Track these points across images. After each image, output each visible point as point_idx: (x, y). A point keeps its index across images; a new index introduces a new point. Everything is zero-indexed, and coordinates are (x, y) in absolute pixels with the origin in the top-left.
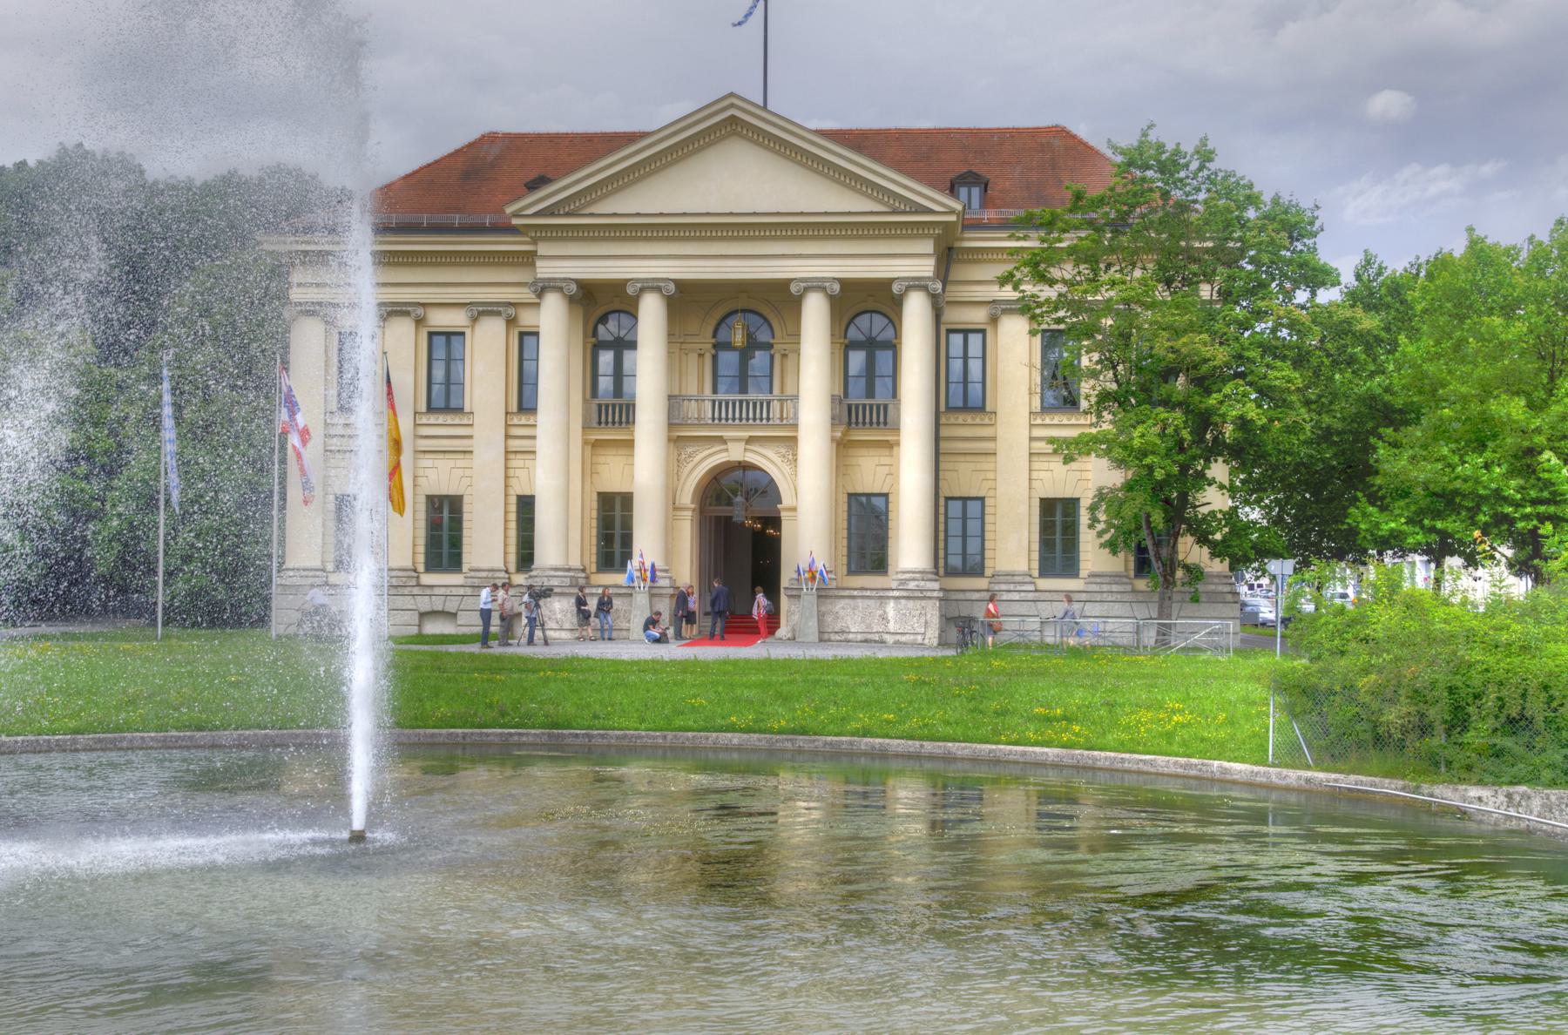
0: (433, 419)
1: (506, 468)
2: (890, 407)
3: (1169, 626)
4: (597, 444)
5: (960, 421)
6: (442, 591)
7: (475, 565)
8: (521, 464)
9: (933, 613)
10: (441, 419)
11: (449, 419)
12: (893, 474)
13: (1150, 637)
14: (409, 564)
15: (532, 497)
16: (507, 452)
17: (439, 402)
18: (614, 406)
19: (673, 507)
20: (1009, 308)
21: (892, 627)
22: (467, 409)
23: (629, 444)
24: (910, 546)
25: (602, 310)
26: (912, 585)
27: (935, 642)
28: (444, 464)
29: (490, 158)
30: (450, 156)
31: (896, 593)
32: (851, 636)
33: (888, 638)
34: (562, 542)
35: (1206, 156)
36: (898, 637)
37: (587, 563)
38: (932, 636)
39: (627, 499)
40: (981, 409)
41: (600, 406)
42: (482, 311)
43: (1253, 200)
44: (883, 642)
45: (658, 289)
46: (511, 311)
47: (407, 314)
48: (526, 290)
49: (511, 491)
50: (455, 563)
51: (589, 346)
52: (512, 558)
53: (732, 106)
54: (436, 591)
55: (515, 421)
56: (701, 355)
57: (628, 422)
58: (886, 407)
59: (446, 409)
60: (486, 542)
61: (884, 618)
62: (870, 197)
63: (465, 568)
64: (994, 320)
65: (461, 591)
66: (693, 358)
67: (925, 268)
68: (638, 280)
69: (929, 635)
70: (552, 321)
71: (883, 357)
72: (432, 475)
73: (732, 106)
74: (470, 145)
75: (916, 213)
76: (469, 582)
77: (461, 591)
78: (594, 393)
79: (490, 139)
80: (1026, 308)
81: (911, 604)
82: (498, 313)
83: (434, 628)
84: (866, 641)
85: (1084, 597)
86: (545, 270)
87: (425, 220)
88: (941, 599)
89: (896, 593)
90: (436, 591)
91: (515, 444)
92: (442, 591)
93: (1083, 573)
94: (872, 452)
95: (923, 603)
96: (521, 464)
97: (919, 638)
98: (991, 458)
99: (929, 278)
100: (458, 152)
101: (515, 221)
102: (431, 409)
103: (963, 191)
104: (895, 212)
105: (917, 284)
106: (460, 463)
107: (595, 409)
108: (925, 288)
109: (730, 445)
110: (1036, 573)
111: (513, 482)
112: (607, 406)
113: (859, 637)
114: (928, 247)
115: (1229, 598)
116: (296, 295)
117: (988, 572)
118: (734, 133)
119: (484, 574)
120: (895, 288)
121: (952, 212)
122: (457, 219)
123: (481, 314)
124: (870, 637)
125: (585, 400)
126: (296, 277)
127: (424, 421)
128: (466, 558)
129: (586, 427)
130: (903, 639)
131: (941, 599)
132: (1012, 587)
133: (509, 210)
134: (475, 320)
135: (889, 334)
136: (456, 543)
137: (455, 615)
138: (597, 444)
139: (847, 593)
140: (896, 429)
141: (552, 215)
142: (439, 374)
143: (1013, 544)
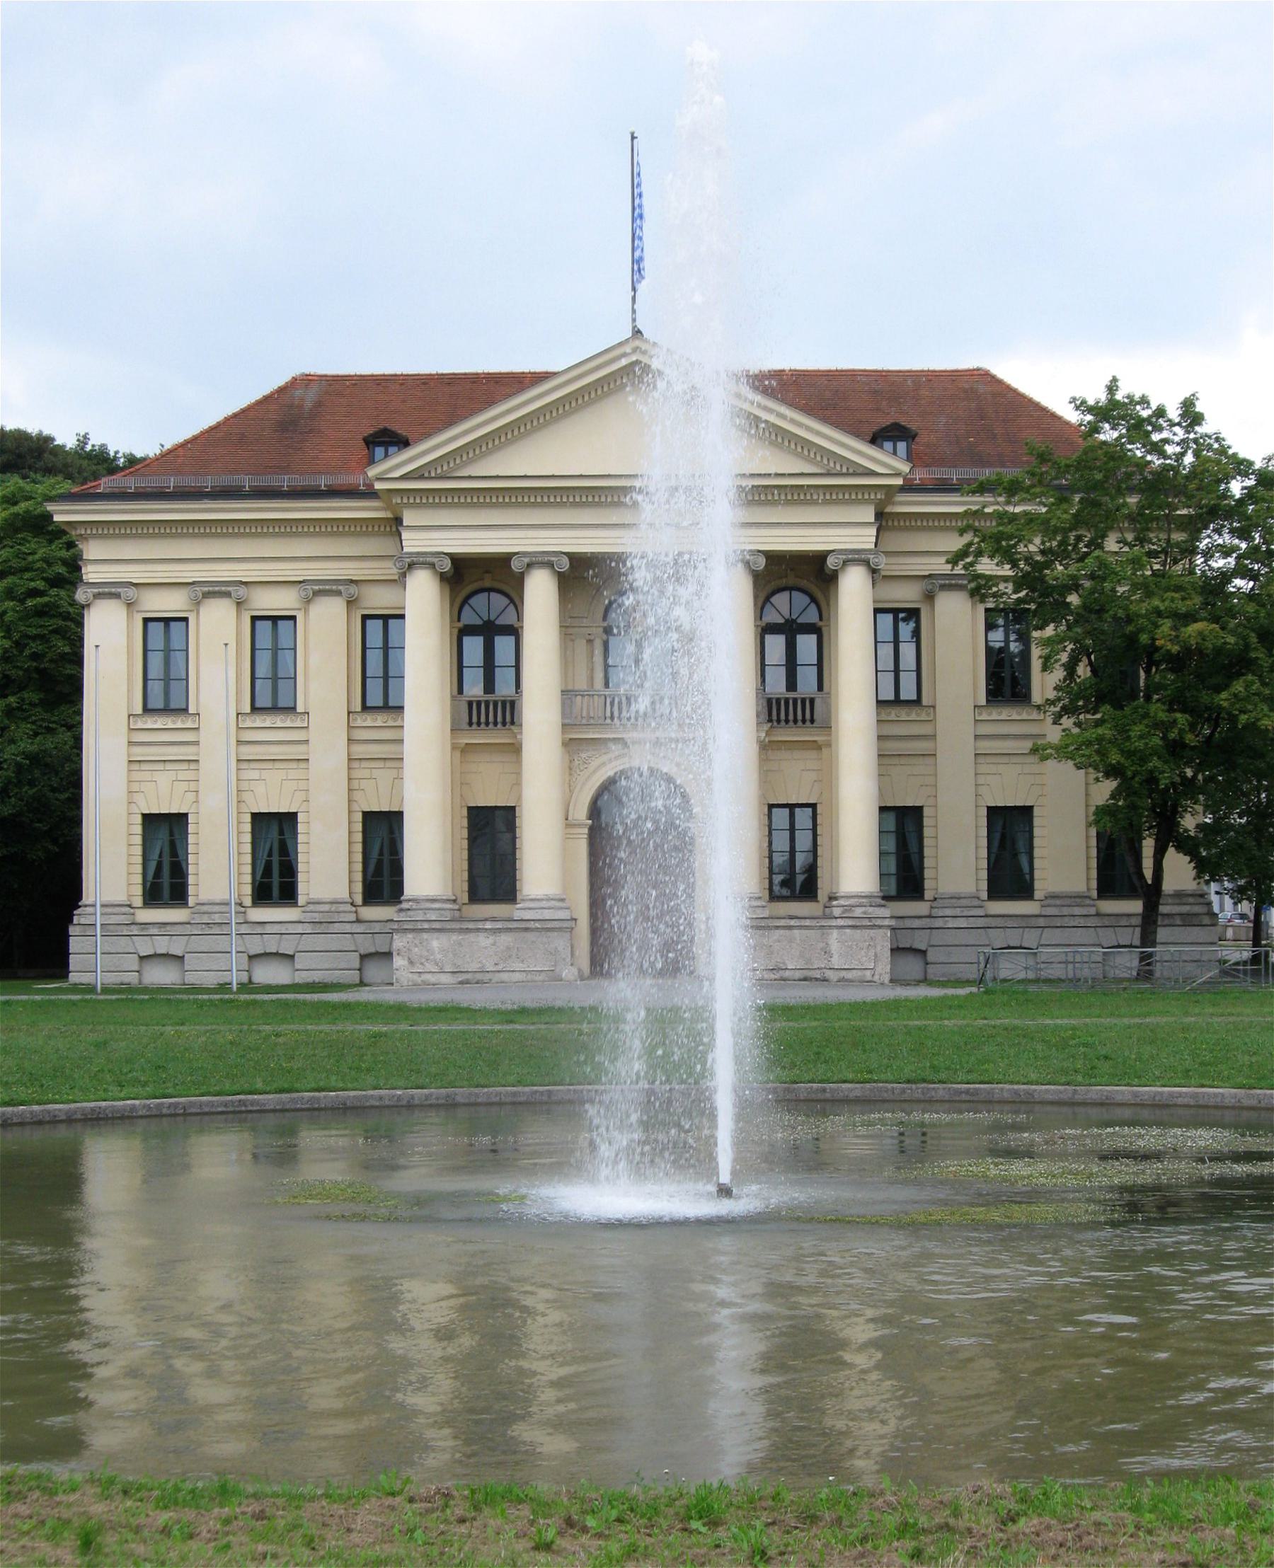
0: (259, 721)
1: (349, 779)
2: (818, 703)
3: (1150, 955)
4: (467, 750)
5: (893, 717)
6: (276, 929)
8: (366, 773)
9: (883, 941)
10: (268, 720)
11: (279, 720)
12: (828, 777)
13: (1128, 963)
14: (344, 895)
15: (399, 815)
16: (349, 760)
17: (264, 700)
18: (487, 703)
19: (569, 823)
20: (949, 584)
21: (836, 962)
22: (300, 709)
23: (515, 749)
24: (855, 864)
26: (858, 912)
27: (886, 979)
28: (274, 776)
29: (308, 404)
30: (258, 403)
31: (841, 922)
32: (787, 974)
34: (430, 863)
35: (1191, 415)
36: (843, 974)
37: (459, 894)
38: (884, 969)
39: (509, 814)
40: (918, 702)
41: (470, 704)
43: (1241, 467)
44: (825, 980)
45: (550, 565)
46: (353, 589)
47: (228, 595)
48: (389, 564)
49: (356, 807)
50: (288, 894)
51: (456, 632)
52: (359, 887)
54: (269, 929)
55: (359, 722)
56: (590, 642)
57: (513, 723)
58: (812, 701)
59: (275, 709)
60: (327, 864)
61: (827, 952)
62: (799, 456)
63: (301, 900)
64: (930, 597)
65: (300, 929)
66: (581, 645)
67: (865, 538)
68: (525, 554)
69: (879, 970)
70: (423, 603)
71: (806, 644)
72: (260, 789)
74: (281, 390)
75: (855, 474)
76: (308, 917)
77: (300, 929)
78: (460, 691)
79: (305, 381)
80: (979, 588)
82: (339, 593)
83: (268, 974)
84: (805, 979)
85: (1041, 922)
86: (413, 542)
87: (247, 482)
88: (893, 929)
89: (841, 922)
90: (269, 929)
91: (359, 750)
92: (276, 929)
93: (1038, 894)
94: (797, 754)
95: (872, 932)
96: (366, 773)
97: (868, 973)
98: (930, 760)
99: (870, 550)
100: (267, 399)
101: (378, 486)
102: (255, 709)
103: (888, 445)
104: (828, 474)
105: (855, 558)
106: (292, 774)
107: (465, 708)
108: (866, 563)
110: (985, 895)
111: (357, 796)
112: (479, 703)
113: (798, 975)
114: (868, 514)
115: (1206, 920)
116: (91, 574)
117: (928, 895)
119: (326, 908)
120: (831, 562)
121: (898, 474)
122: (285, 482)
123: (317, 593)
125: (453, 697)
126: (92, 550)
127: (248, 724)
128: (301, 888)
129: (455, 729)
130: (849, 975)
131: (893, 929)
132: (958, 912)
133: (372, 472)
134: (308, 601)
135: (811, 616)
136: (289, 870)
137: (292, 957)
138: (467, 750)
139: (782, 923)
140: (827, 727)
141: (422, 478)
142: (263, 669)
143: (957, 860)
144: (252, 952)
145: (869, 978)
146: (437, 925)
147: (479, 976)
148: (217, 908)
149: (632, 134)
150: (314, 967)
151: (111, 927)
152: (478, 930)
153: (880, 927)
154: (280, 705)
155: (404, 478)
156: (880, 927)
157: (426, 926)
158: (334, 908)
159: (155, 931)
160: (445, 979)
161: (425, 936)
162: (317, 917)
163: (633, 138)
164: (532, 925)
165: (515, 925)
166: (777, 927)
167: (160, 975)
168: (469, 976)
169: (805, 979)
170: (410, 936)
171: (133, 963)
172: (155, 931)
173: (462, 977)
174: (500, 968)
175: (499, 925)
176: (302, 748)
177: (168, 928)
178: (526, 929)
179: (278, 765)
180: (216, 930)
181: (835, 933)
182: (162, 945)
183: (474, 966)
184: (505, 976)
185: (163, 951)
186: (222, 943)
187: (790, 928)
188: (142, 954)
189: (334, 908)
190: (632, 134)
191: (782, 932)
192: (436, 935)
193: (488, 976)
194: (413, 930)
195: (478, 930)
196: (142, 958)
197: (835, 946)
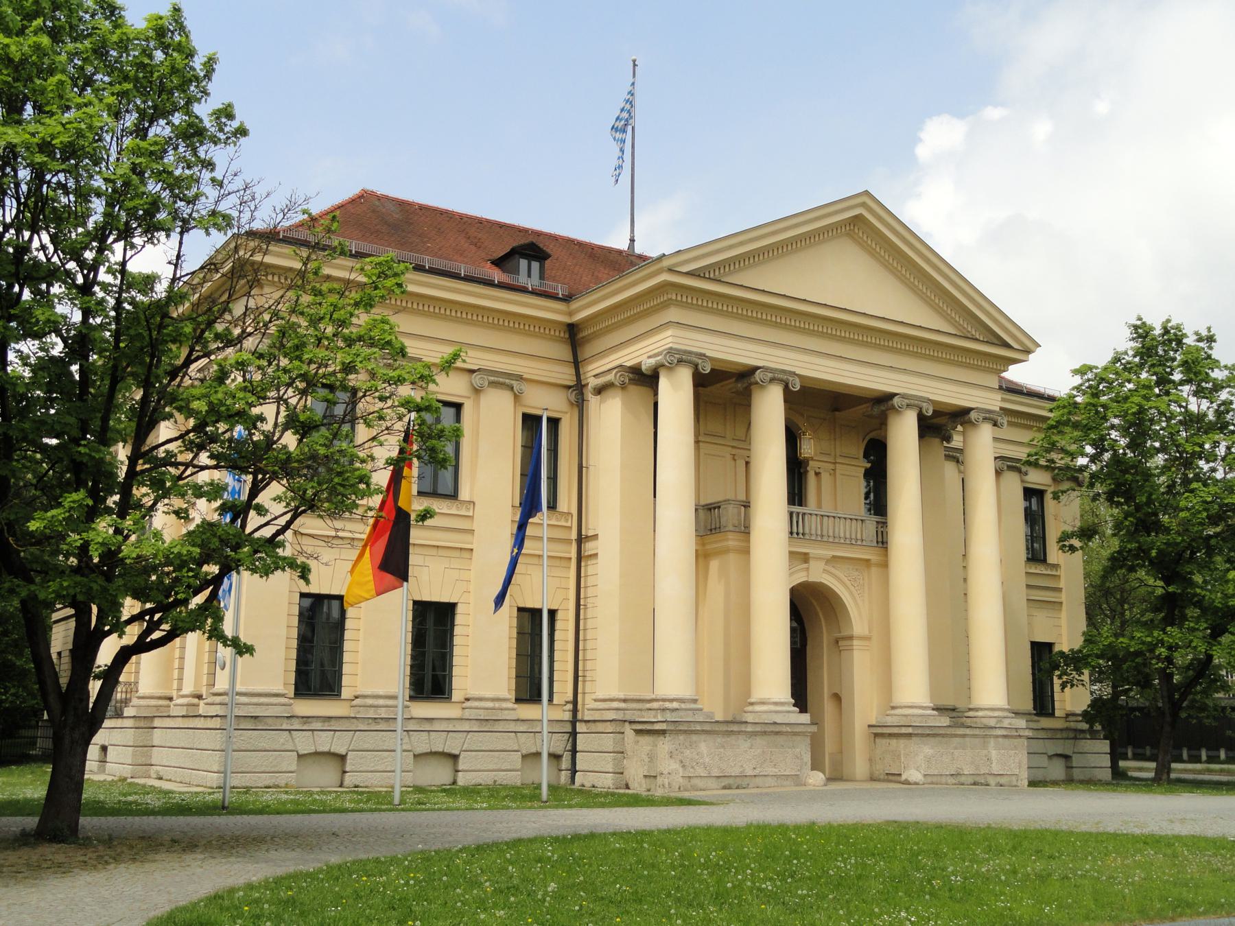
7: (473, 693)
21: (996, 769)
25: (723, 394)
26: (1006, 723)
31: (999, 732)
32: (963, 779)
33: (992, 781)
42: (506, 382)
53: (864, 205)
54: (437, 726)
73: (864, 205)
81: (1006, 741)
89: (999, 732)
95: (1016, 741)
97: (1014, 778)
109: (813, 564)
113: (970, 780)
118: (850, 235)
119: (490, 704)
124: (978, 779)
134: (477, 391)
144: (419, 750)
145: (1014, 783)
146: (707, 727)
147: (739, 781)
148: (381, 702)
149: (634, 61)
150: (479, 767)
151: (270, 721)
152: (739, 732)
153: (1020, 736)
154: (440, 491)
155: (690, 274)
156: (1020, 736)
157: (698, 728)
158: (497, 705)
159: (318, 725)
160: (712, 783)
161: (694, 737)
162: (483, 715)
163: (635, 65)
164: (784, 729)
165: (772, 728)
166: (956, 736)
167: (321, 778)
168: (731, 781)
169: (975, 784)
170: (681, 737)
171: (290, 762)
172: (318, 725)
173: (726, 782)
174: (756, 772)
175: (758, 729)
176: (467, 537)
177: (333, 722)
178: (777, 733)
179: (441, 552)
180: (382, 726)
181: (992, 741)
182: (325, 742)
183: (736, 771)
184: (758, 781)
185: (326, 749)
186: (388, 740)
187: (964, 736)
188: (301, 752)
189: (497, 705)
190: (634, 61)
191: (957, 740)
192: (703, 737)
193: (746, 781)
194: (685, 732)
195: (739, 732)
196: (300, 756)
197: (994, 753)
